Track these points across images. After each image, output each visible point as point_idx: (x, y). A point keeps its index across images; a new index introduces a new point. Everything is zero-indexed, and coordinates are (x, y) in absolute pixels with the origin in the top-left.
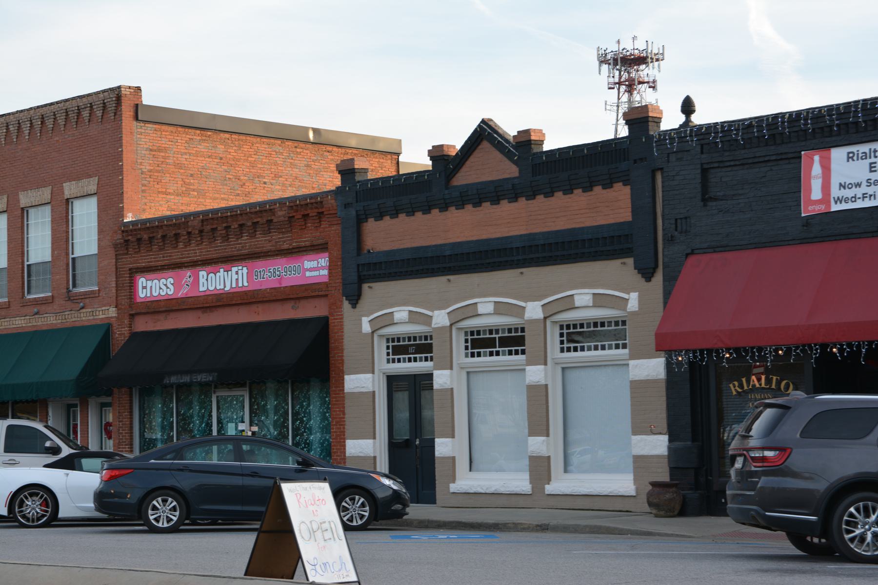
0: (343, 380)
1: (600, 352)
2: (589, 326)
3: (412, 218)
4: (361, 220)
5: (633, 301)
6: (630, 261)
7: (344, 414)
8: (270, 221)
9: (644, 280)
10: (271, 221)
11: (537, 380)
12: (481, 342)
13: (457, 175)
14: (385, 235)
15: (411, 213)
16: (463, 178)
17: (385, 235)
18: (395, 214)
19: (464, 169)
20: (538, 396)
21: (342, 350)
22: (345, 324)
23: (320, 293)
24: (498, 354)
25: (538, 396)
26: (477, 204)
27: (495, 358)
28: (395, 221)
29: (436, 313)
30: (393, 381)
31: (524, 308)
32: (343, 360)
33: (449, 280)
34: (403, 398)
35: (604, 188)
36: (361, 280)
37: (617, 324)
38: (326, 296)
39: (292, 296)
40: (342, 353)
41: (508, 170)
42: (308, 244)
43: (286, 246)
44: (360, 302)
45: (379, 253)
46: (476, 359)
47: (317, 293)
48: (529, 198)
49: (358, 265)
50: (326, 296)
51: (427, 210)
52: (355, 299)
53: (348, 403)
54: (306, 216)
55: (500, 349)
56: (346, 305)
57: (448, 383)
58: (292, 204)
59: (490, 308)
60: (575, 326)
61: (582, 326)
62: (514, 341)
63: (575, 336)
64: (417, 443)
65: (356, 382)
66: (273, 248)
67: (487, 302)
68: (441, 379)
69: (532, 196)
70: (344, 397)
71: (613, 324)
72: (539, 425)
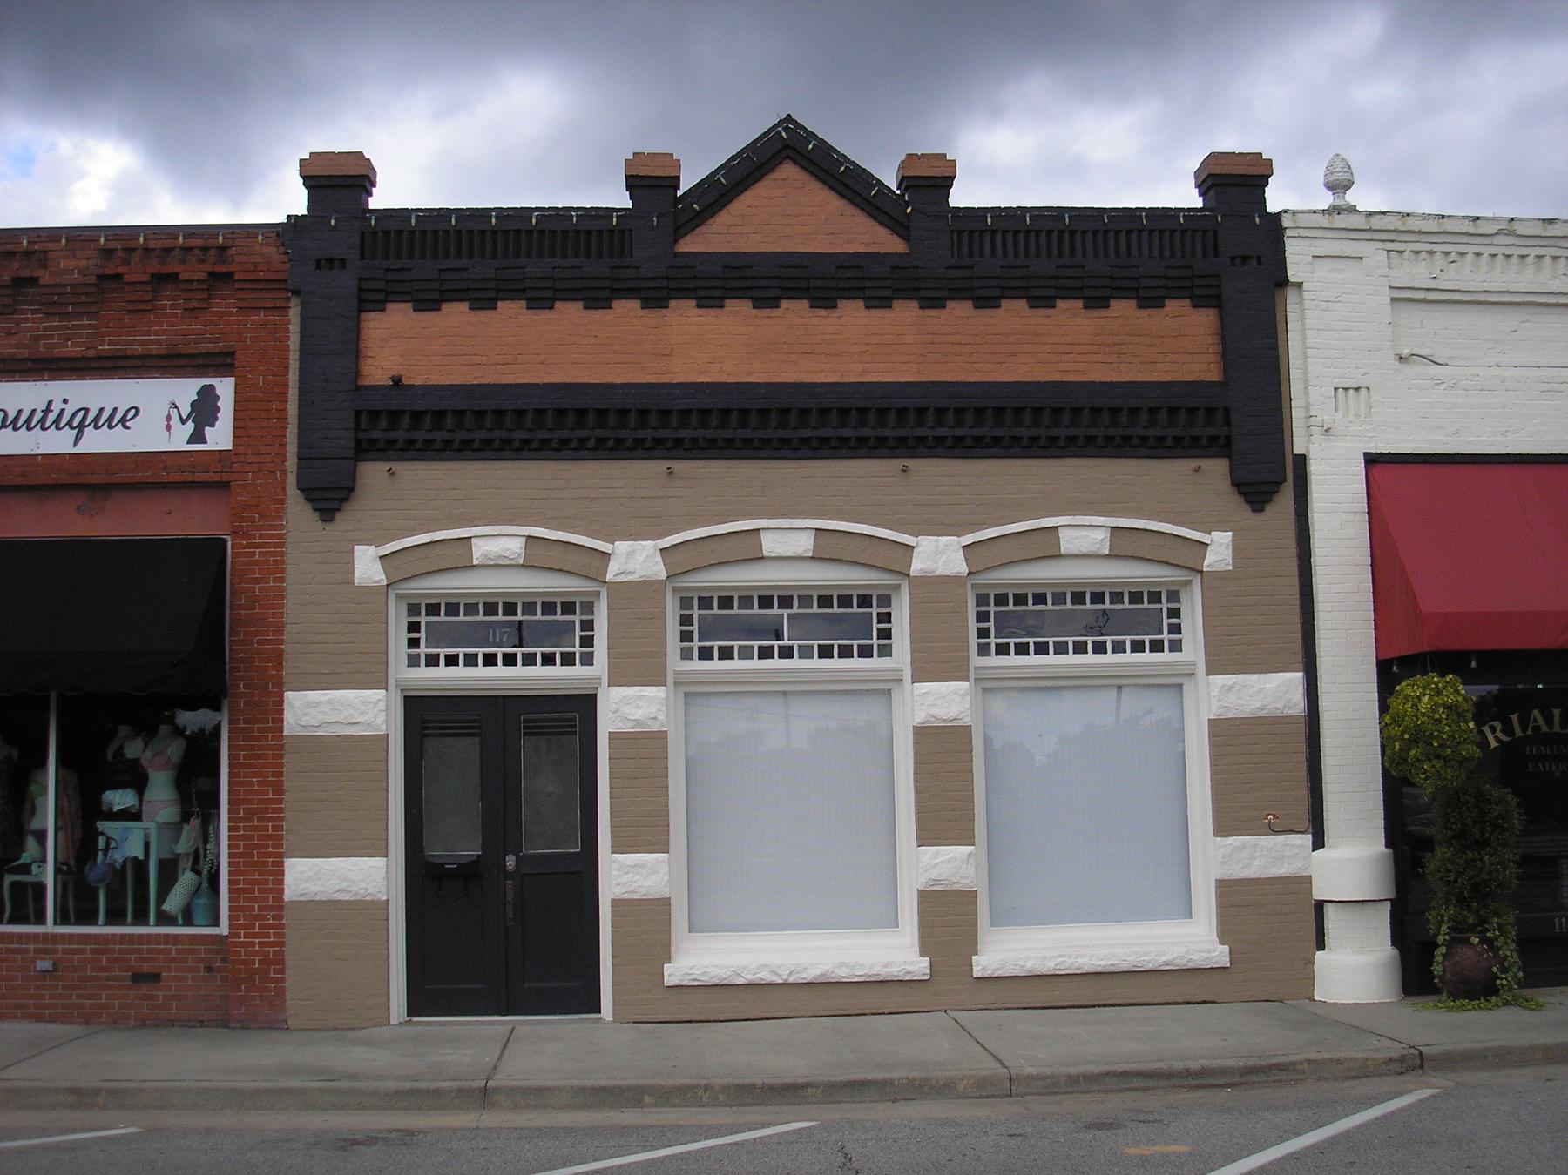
0: (281, 702)
1: (1090, 658)
2: (1059, 598)
3: (545, 315)
4: (372, 298)
5: (1219, 549)
6: (1217, 468)
7: (279, 790)
8: (21, 283)
9: (1248, 507)
10: (33, 281)
11: (952, 715)
12: (732, 621)
13: (697, 231)
14: (409, 347)
15: (541, 299)
16: (715, 237)
17: (409, 347)
18: (483, 299)
19: (723, 219)
20: (942, 749)
21: (280, 628)
22: (289, 558)
23: (199, 477)
24: (786, 653)
25: (942, 749)
26: (766, 300)
27: (776, 663)
28: (484, 316)
29: (622, 547)
30: (426, 717)
31: (910, 548)
32: (280, 653)
33: (670, 472)
34: (460, 758)
35: (1140, 307)
36: (365, 449)
37: (1136, 597)
38: (224, 486)
39: (89, 479)
40: (281, 632)
41: (864, 236)
42: (154, 349)
43: (71, 350)
44: (347, 506)
45: (428, 389)
46: (716, 664)
47: (187, 477)
48: (759, 303)
49: (358, 413)
50: (224, 486)
51: (598, 298)
52: (330, 497)
53: (291, 763)
54: (162, 280)
55: (796, 644)
56: (298, 513)
57: (662, 717)
58: (111, 245)
59: (803, 544)
60: (1020, 599)
61: (1040, 598)
62: (849, 621)
63: (1015, 618)
64: (511, 862)
65: (310, 710)
66: (26, 353)
67: (788, 536)
68: (624, 708)
69: (933, 302)
70: (281, 747)
71: (1126, 599)
72: (944, 819)
